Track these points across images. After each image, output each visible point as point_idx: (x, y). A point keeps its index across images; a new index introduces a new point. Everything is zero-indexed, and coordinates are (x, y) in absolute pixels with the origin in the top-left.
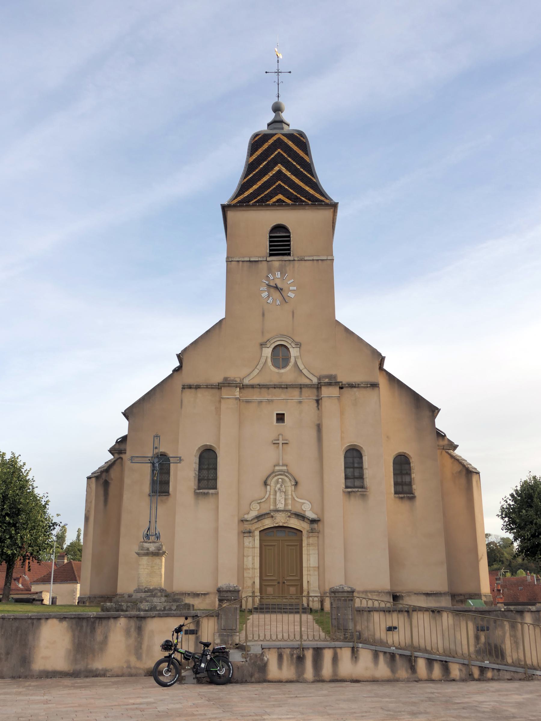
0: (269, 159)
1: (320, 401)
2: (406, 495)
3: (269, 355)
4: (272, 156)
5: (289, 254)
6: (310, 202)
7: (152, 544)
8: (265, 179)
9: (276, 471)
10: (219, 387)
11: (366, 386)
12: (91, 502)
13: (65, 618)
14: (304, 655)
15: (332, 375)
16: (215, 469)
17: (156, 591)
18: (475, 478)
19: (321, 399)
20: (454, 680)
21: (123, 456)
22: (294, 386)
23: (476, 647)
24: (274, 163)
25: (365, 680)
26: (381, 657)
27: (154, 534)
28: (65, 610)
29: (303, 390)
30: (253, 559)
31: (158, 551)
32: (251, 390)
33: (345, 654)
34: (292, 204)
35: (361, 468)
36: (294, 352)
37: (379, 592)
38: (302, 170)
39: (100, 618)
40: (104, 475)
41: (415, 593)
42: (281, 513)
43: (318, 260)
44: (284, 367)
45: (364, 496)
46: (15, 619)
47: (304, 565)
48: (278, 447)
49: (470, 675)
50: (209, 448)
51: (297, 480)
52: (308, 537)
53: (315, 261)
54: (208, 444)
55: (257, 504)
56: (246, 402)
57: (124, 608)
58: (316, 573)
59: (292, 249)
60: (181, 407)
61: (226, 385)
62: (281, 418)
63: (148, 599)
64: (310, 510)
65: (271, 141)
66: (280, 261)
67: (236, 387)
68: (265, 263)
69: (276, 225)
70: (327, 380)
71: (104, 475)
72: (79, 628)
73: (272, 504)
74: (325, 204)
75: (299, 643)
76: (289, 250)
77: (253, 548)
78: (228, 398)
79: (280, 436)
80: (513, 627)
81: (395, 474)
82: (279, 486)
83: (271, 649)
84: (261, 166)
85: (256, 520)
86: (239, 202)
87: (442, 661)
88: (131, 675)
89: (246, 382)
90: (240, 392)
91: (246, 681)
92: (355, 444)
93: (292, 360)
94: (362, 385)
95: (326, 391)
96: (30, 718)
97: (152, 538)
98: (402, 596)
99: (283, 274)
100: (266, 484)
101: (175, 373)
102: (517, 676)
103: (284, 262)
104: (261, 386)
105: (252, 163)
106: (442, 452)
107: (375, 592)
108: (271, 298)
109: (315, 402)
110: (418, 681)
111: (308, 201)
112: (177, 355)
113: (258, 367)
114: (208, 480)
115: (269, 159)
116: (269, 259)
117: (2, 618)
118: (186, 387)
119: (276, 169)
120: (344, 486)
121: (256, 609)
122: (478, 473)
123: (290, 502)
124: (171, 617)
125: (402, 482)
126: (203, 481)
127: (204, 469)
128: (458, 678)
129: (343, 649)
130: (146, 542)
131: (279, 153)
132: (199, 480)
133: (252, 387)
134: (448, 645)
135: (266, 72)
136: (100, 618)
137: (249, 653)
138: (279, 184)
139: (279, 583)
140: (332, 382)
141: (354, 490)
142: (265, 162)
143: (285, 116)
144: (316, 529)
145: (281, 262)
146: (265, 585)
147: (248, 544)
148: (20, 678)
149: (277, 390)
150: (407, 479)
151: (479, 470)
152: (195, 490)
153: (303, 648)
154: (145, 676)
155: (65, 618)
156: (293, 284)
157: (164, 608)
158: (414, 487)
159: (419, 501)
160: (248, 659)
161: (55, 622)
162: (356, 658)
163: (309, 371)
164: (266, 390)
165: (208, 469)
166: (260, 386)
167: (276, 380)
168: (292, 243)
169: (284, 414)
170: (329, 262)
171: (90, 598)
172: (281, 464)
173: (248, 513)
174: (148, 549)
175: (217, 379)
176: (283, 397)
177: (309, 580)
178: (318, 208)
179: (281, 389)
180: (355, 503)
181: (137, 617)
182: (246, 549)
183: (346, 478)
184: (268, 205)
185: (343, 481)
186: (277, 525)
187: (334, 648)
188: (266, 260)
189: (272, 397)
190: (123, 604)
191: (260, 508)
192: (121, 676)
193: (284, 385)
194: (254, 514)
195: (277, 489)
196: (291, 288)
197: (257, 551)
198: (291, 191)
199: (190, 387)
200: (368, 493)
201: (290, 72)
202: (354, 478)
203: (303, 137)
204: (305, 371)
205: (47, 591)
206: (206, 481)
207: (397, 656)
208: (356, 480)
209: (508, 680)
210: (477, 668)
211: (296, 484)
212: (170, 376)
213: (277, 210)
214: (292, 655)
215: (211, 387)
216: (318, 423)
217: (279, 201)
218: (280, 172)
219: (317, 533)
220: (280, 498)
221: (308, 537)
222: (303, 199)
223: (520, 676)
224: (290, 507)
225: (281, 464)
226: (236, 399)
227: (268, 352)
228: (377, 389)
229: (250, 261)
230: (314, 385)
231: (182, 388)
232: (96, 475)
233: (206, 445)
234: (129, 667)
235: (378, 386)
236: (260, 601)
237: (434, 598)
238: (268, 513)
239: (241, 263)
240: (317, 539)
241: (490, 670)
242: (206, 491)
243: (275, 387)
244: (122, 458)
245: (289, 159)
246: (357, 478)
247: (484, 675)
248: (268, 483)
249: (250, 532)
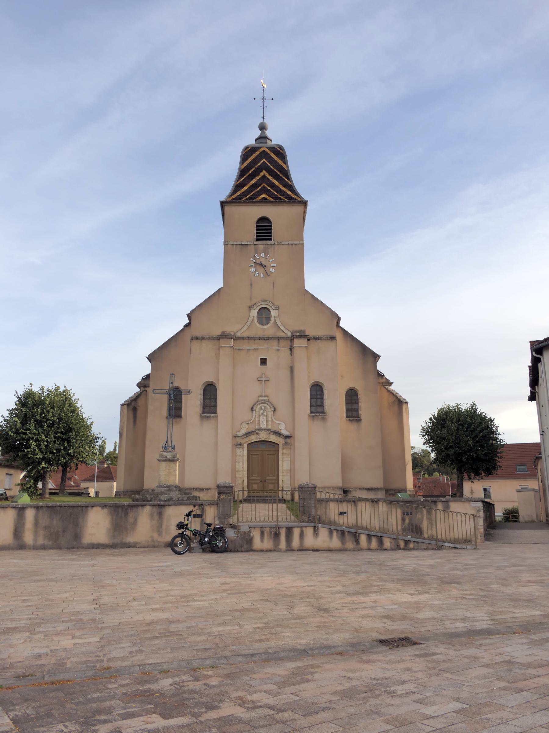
0: (256, 166)
1: (293, 350)
2: (354, 419)
3: (256, 315)
4: (259, 164)
5: (271, 240)
6: (287, 200)
7: (169, 453)
8: (253, 182)
9: (260, 400)
10: (218, 338)
11: (326, 338)
12: (124, 423)
13: (106, 506)
14: (279, 532)
15: (301, 330)
16: (216, 399)
17: (172, 487)
18: (404, 406)
19: (294, 348)
20: (386, 550)
21: (147, 389)
22: (274, 338)
23: (402, 526)
24: (260, 169)
25: (323, 549)
26: (335, 533)
27: (171, 446)
28: (106, 501)
29: (280, 341)
30: (243, 464)
31: (172, 458)
32: (242, 341)
33: (309, 532)
34: (273, 201)
35: (322, 398)
36: (274, 313)
37: (334, 488)
38: (281, 175)
39: (131, 506)
40: (133, 403)
41: (360, 489)
42: (263, 431)
43: (292, 244)
44: (266, 324)
45: (324, 419)
46: (69, 507)
47: (280, 468)
48: (261, 383)
49: (397, 546)
50: (211, 384)
51: (275, 407)
52: (283, 449)
53: (290, 245)
54: (210, 380)
56: (238, 349)
57: (149, 499)
58: (289, 474)
59: (273, 236)
60: (190, 353)
61: (223, 337)
62: (264, 361)
63: (166, 492)
64: (285, 429)
65: (258, 153)
66: (264, 244)
67: (231, 338)
68: (252, 246)
70: (298, 334)
71: (133, 403)
72: (116, 513)
73: (257, 424)
74: (298, 202)
75: (276, 523)
76: (271, 236)
77: (242, 456)
78: (225, 347)
79: (263, 375)
80: (429, 512)
81: (346, 403)
82: (262, 411)
83: (256, 528)
84: (250, 172)
85: (245, 436)
86: (233, 199)
87: (378, 536)
88: (154, 547)
89: (238, 335)
90: (234, 342)
91: (238, 550)
92: (318, 381)
93: (273, 319)
94: (324, 338)
95: (297, 342)
96: (81, 577)
97: (169, 449)
98: (350, 491)
99: (266, 255)
100: (252, 410)
101: (186, 327)
102: (430, 546)
103: (267, 245)
104: (249, 338)
105: (243, 169)
106: (381, 387)
107: (331, 488)
108: (257, 272)
109: (289, 350)
110: (361, 550)
111: (285, 199)
112: (187, 314)
113: (247, 324)
114: (210, 406)
115: (256, 166)
116: (256, 243)
117: (60, 506)
118: (193, 338)
119: (262, 174)
120: (310, 412)
121: (245, 500)
122: (407, 403)
123: (270, 423)
124: (184, 505)
125: (352, 409)
126: (206, 408)
127: (208, 399)
128: (389, 548)
129: (307, 528)
130: (165, 452)
131: (264, 162)
132: (204, 407)
133: (243, 338)
134: (382, 525)
135: (254, 99)
136: (131, 506)
137: (240, 530)
138: (264, 186)
139: (261, 481)
140: (302, 335)
141: (317, 414)
142: (253, 169)
143: (268, 133)
144: (289, 442)
145: (265, 245)
146: (251, 483)
147: (239, 453)
148: (73, 548)
149: (261, 342)
150: (355, 407)
151: (407, 400)
152: (201, 414)
153: (279, 527)
154: (165, 547)
155: (106, 506)
156: (273, 262)
157: (178, 499)
158: (360, 412)
159: (364, 423)
160: (239, 535)
161: (99, 509)
162: (316, 534)
163: (285, 327)
164: (253, 341)
165: (210, 399)
166: (249, 338)
167: (260, 334)
168: (273, 231)
169: (266, 359)
170: (300, 245)
171: (123, 492)
172: (263, 395)
173: (239, 431)
174: (166, 457)
175: (217, 332)
176: (266, 346)
177: (283, 479)
178: (293, 204)
179: (264, 340)
180: (317, 424)
181: (159, 506)
182: (237, 457)
183: (311, 406)
184: (256, 202)
185: (309, 408)
186: (260, 440)
187: (301, 527)
188: (254, 244)
189: (257, 346)
190: (148, 496)
192: (147, 547)
193: (266, 337)
194: (243, 432)
195: (260, 413)
196: (272, 265)
197: (246, 458)
198: (273, 191)
199: (197, 338)
200: (327, 417)
201: (272, 99)
202: (317, 406)
203: (282, 150)
204: (282, 327)
205: (92, 487)
206: (208, 408)
207: (346, 533)
208: (318, 407)
209: (424, 549)
210: (403, 541)
211: (275, 410)
212: (182, 331)
213: (262, 205)
214: (271, 532)
215: (212, 338)
216: (291, 365)
217: (264, 199)
218: (264, 176)
219: (289, 446)
220: (263, 421)
221: (283, 449)
222: (282, 197)
223: (433, 546)
224: (270, 427)
225: (263, 395)
226: (231, 347)
227: (254, 313)
228: (335, 340)
229: (241, 244)
230: (288, 337)
231: (191, 339)
232: (126, 403)
233: (209, 381)
234: (153, 541)
235: (335, 338)
236: (248, 494)
237: (373, 492)
238: (254, 431)
239: (235, 246)
240: (289, 450)
241: (412, 543)
242: (208, 415)
243: (260, 339)
244: (146, 391)
245: (271, 166)
246: (319, 406)
247: (408, 546)
249: (240, 445)
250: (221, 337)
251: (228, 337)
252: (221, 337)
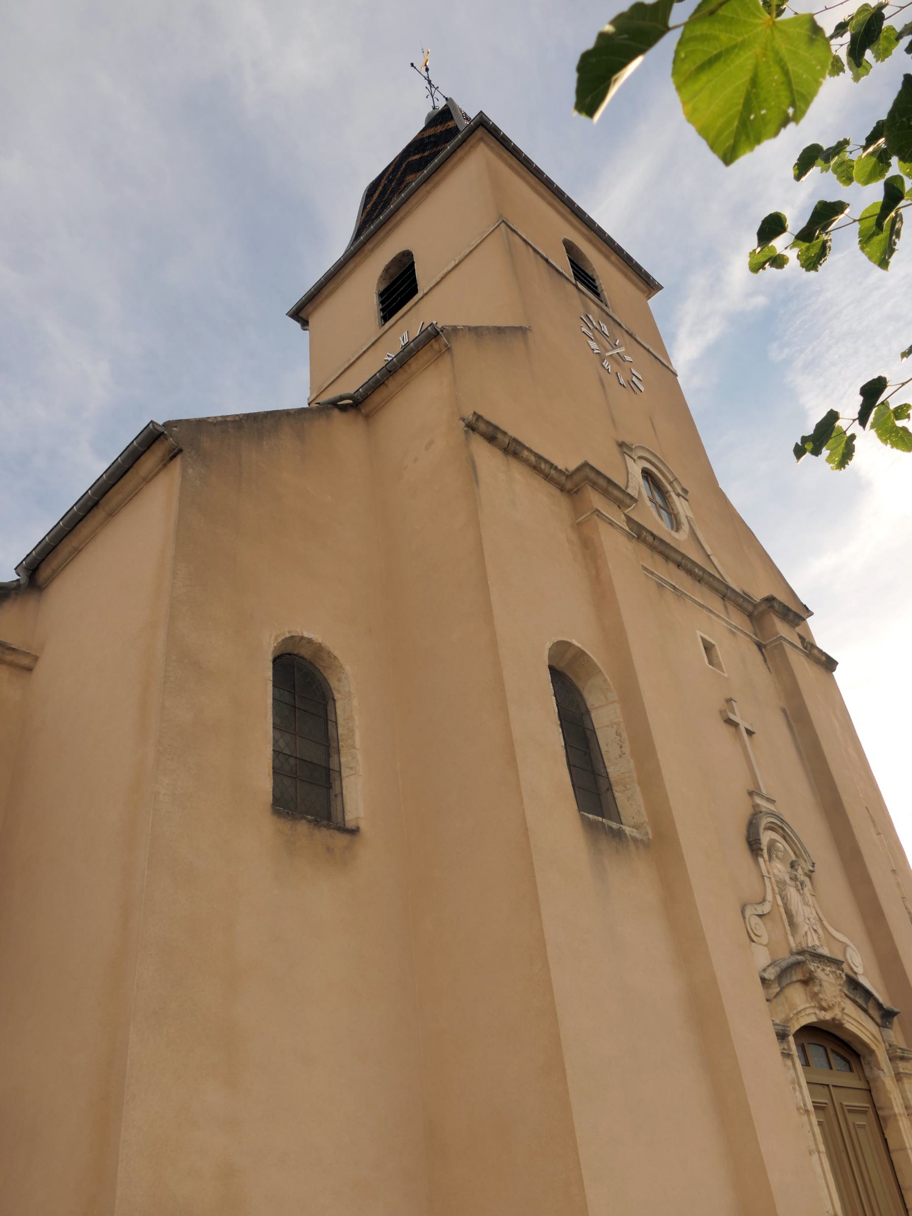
69: (569, 240)
118: (482, 426)
250: (592, 475)
251: (616, 493)
252: (592, 475)
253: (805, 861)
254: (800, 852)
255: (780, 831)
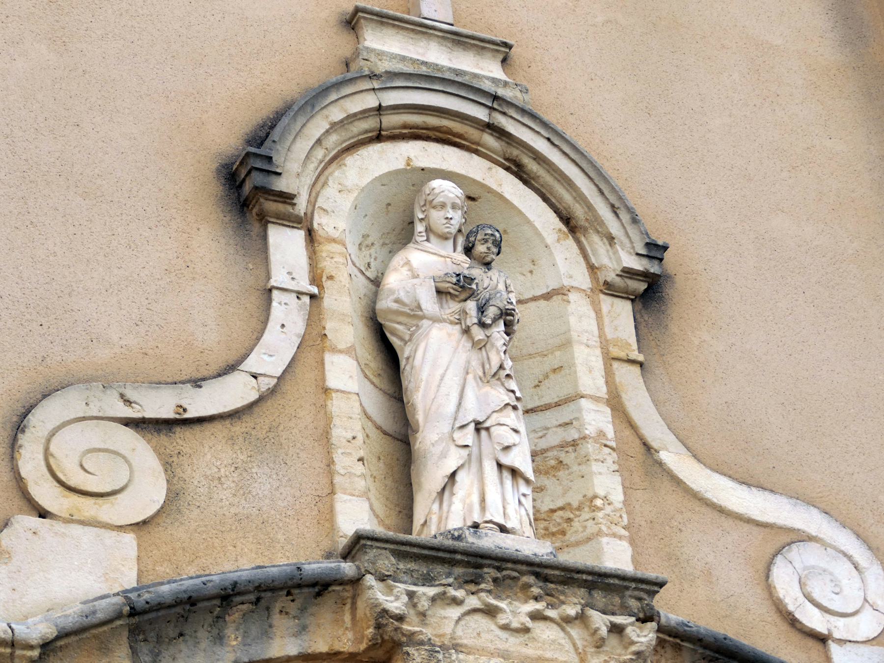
55: (128, 439)
191: (173, 497)
248: (282, 185)
253: (611, 239)
254: (590, 207)
255: (489, 140)
